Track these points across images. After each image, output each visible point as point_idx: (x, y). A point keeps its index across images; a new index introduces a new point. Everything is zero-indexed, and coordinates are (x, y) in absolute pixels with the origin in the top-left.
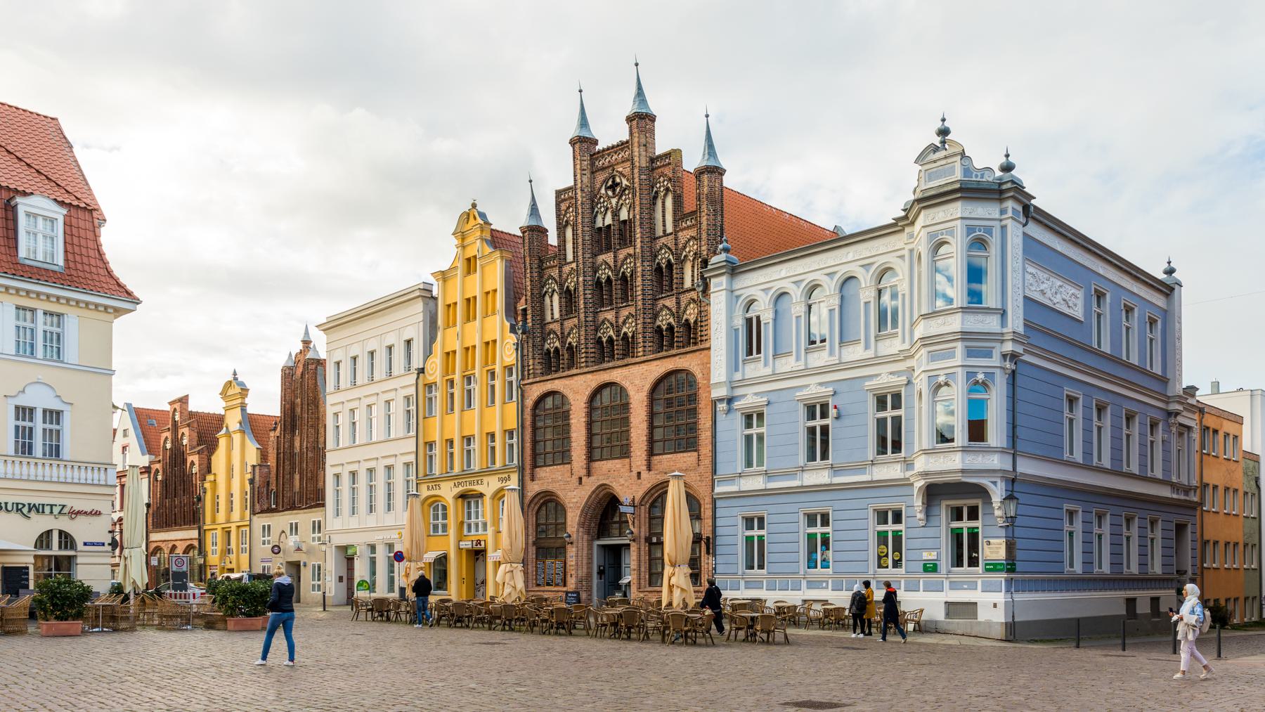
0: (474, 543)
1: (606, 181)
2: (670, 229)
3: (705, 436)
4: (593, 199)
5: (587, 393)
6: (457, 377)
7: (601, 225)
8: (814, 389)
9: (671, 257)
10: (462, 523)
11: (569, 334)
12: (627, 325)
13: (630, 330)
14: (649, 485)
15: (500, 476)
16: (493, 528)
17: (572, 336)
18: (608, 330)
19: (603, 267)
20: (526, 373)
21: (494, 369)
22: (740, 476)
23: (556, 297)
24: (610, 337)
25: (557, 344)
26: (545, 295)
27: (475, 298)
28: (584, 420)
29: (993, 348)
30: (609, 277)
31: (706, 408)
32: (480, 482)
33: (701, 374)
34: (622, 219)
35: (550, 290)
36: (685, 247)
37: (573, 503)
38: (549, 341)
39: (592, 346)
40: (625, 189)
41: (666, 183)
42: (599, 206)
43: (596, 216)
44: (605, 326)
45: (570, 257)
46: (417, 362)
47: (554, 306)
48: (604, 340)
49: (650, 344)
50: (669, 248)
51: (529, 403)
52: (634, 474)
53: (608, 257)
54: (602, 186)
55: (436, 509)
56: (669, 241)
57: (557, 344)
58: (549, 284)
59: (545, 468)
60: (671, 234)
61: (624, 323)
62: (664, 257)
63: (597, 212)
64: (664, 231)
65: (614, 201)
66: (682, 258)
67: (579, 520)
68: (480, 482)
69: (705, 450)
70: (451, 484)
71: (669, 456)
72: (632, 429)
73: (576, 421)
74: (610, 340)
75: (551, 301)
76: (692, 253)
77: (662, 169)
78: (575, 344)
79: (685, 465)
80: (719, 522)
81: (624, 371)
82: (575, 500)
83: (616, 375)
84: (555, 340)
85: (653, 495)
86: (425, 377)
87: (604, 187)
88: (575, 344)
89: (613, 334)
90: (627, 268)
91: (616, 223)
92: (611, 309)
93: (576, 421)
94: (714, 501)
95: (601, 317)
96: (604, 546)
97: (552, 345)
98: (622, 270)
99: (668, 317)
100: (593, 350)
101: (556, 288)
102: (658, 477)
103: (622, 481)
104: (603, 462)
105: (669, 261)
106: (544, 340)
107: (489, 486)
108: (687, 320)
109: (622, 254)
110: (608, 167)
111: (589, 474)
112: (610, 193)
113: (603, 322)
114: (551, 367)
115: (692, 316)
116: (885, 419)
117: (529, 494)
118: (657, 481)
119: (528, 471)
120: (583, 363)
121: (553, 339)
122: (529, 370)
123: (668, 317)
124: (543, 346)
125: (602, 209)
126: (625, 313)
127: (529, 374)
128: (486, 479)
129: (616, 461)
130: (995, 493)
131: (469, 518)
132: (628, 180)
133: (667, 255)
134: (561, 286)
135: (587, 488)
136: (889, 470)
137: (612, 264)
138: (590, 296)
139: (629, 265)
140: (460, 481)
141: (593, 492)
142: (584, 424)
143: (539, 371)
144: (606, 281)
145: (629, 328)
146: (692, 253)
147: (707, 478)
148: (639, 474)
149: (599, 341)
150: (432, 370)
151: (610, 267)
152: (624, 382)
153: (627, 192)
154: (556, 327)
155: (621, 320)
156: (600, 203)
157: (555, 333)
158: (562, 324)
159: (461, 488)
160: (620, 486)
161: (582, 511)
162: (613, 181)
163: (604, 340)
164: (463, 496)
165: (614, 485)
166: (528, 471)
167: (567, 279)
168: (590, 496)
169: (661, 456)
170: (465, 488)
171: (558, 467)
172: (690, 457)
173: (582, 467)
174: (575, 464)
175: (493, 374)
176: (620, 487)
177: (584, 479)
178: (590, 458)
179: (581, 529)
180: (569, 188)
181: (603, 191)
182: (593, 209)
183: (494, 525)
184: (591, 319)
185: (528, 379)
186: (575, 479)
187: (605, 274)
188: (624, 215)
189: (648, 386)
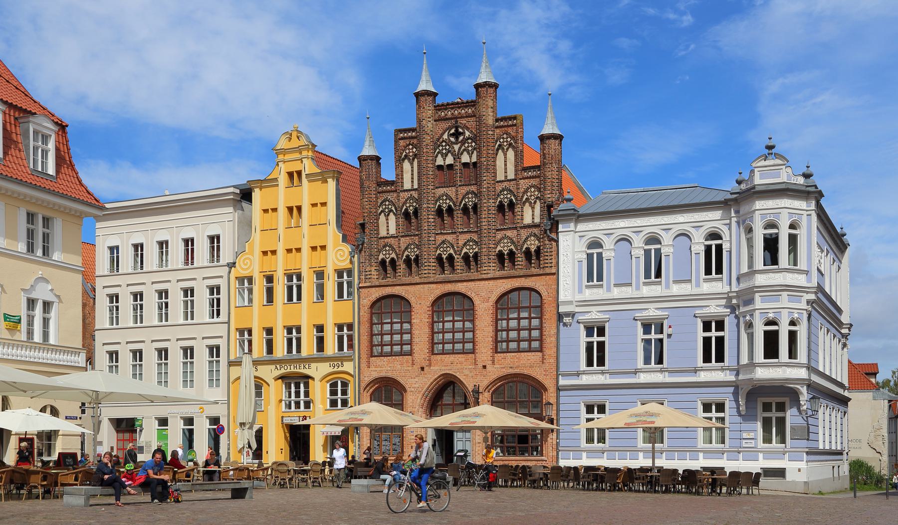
1: (450, 128)
2: (511, 175)
3: (549, 341)
7: (442, 163)
8: (652, 312)
9: (513, 198)
13: (471, 251)
14: (495, 377)
17: (409, 250)
19: (445, 198)
20: (363, 277)
21: (324, 270)
22: (584, 373)
23: (392, 217)
24: (450, 255)
26: (380, 214)
27: (299, 209)
29: (802, 296)
31: (551, 319)
32: (307, 366)
33: (546, 292)
34: (463, 161)
35: (387, 210)
36: (526, 192)
41: (509, 139)
42: (441, 148)
43: (437, 156)
45: (407, 185)
46: (226, 256)
47: (389, 225)
48: (444, 257)
49: (494, 265)
50: (511, 191)
51: (367, 302)
52: (480, 366)
53: (451, 191)
54: (445, 132)
56: (512, 186)
57: (393, 255)
58: (385, 205)
60: (511, 180)
62: (505, 198)
64: (506, 177)
65: (456, 147)
66: (524, 199)
68: (307, 366)
69: (550, 351)
70: (273, 367)
71: (513, 354)
75: (387, 219)
76: (533, 198)
77: (506, 129)
78: (413, 258)
79: (529, 362)
80: (562, 407)
82: (417, 386)
83: (461, 287)
84: (391, 252)
85: (496, 384)
87: (447, 133)
88: (413, 258)
89: (453, 253)
90: (469, 201)
91: (458, 164)
92: (452, 233)
94: (559, 389)
97: (387, 256)
98: (464, 202)
99: (509, 244)
101: (393, 209)
102: (504, 370)
103: (467, 372)
105: (511, 201)
107: (318, 371)
108: (528, 249)
111: (430, 365)
112: (452, 139)
114: (387, 274)
115: (533, 246)
116: (710, 338)
118: (502, 373)
123: (509, 244)
125: (444, 151)
126: (463, 239)
128: (313, 365)
130: (802, 393)
133: (509, 196)
136: (714, 374)
137: (453, 196)
138: (433, 220)
141: (436, 379)
144: (446, 210)
145: (469, 249)
146: (533, 198)
147: (552, 373)
148: (484, 367)
150: (245, 264)
151: (451, 199)
152: (469, 293)
154: (392, 241)
155: (461, 243)
156: (442, 146)
157: (390, 246)
159: (283, 371)
160: (464, 376)
162: (457, 130)
163: (444, 257)
165: (457, 375)
167: (405, 203)
169: (505, 354)
170: (288, 370)
171: (397, 357)
172: (534, 356)
176: (465, 377)
179: (420, 409)
181: (445, 136)
186: (417, 367)
187: (446, 203)
188: (465, 158)
189: (494, 298)
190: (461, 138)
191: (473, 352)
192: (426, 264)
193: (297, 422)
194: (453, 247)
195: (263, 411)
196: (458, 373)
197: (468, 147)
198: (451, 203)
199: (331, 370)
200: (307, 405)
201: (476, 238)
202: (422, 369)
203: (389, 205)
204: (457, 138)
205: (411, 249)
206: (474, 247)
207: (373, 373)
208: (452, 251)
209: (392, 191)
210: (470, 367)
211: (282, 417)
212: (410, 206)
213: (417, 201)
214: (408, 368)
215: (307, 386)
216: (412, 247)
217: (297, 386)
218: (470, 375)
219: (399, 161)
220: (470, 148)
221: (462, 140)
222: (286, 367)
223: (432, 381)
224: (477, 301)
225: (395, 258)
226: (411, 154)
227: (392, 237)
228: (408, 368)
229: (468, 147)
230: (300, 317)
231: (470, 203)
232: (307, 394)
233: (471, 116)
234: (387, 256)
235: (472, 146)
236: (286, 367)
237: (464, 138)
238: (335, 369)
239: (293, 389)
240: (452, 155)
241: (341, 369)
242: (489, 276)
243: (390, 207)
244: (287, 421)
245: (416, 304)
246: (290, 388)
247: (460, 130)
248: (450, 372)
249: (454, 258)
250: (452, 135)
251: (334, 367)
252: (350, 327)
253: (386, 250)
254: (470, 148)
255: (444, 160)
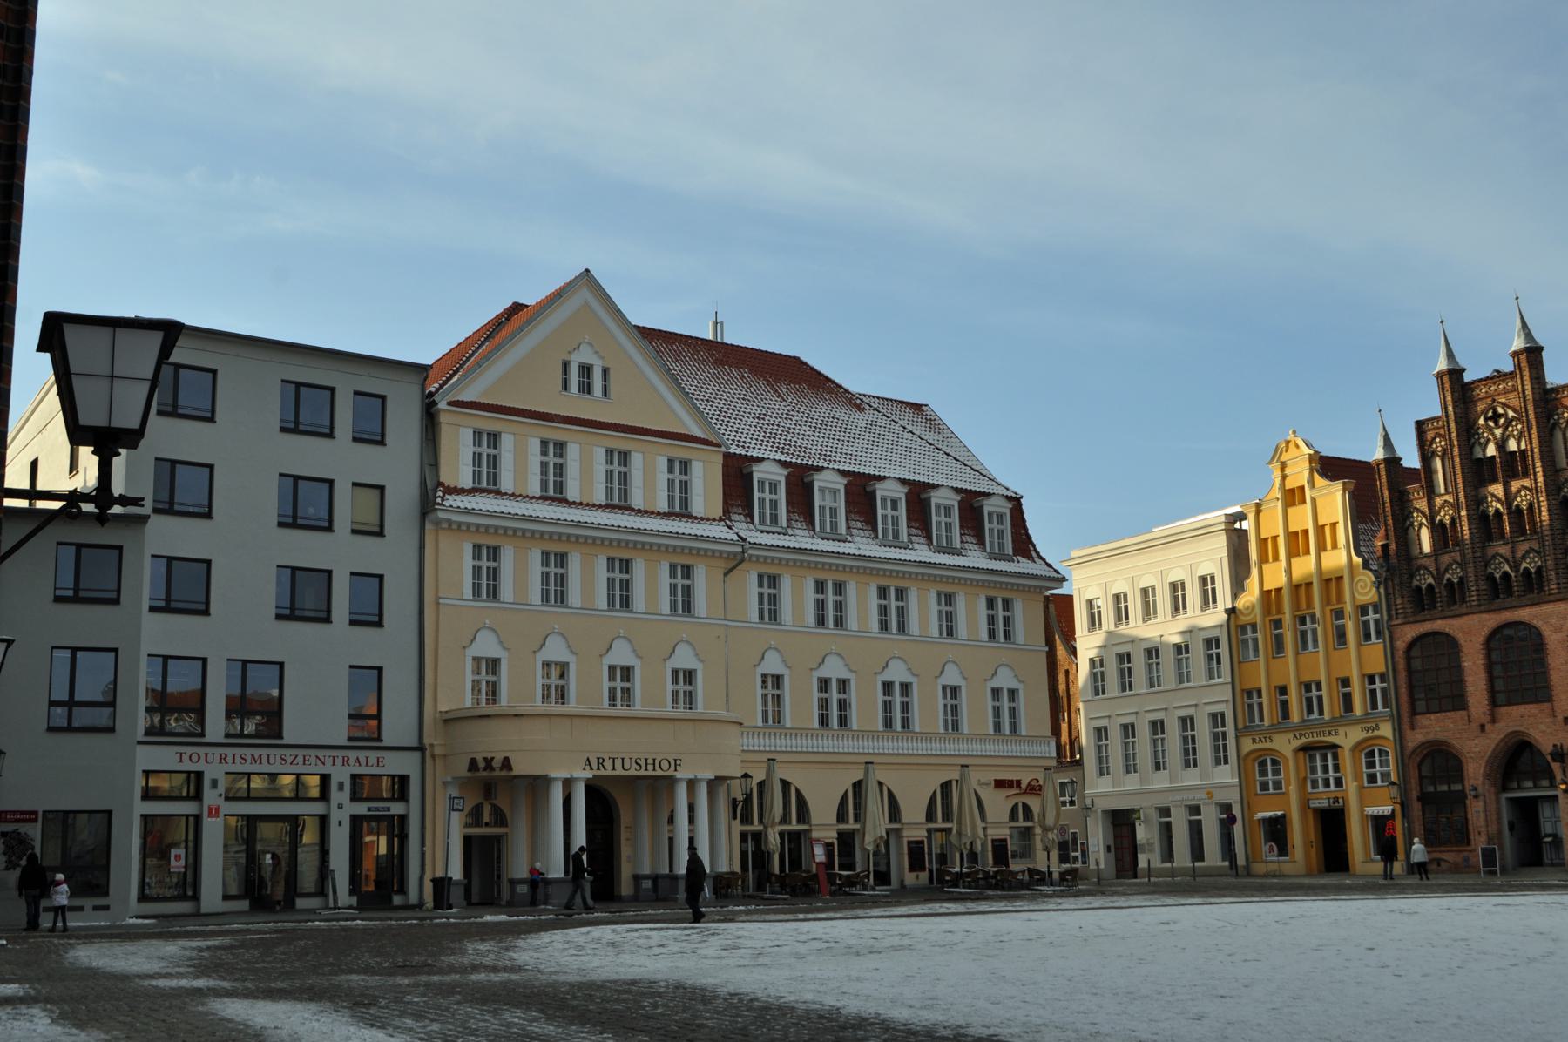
0: (1331, 801)
4: (1468, 432)
5: (1483, 634)
6: (1287, 617)
10: (1305, 779)
11: (1446, 570)
12: (1528, 560)
13: (1533, 565)
15: (1364, 726)
16: (1355, 784)
17: (1450, 572)
18: (1502, 565)
20: (1393, 612)
24: (1506, 575)
25: (1430, 580)
27: (1306, 532)
28: (1482, 662)
30: (1497, 510)
37: (1474, 753)
38: (1418, 578)
39: (1482, 583)
40: (1512, 421)
43: (1473, 446)
44: (1497, 561)
48: (1498, 576)
51: (1401, 645)
55: (1263, 764)
57: (1430, 580)
59: (1429, 715)
61: (1524, 558)
63: (1474, 443)
65: (1498, 432)
67: (1485, 771)
70: (1291, 736)
72: (1551, 672)
73: (1470, 664)
74: (1506, 575)
78: (1456, 581)
81: (1536, 610)
82: (1477, 750)
83: (1523, 614)
84: (1426, 576)
86: (1237, 617)
88: (1456, 581)
90: (1522, 501)
93: (1470, 664)
95: (1491, 552)
96: (1511, 799)
97: (1423, 582)
100: (1485, 587)
101: (1424, 521)
103: (1543, 727)
104: (1511, 707)
106: (1412, 576)
107: (1348, 738)
109: (1515, 485)
110: (1486, 398)
111: (1494, 721)
112: (1491, 424)
113: (1494, 557)
117: (1410, 744)
119: (1406, 719)
120: (1473, 601)
121: (1424, 574)
122: (1396, 610)
124: (1411, 582)
125: (1482, 440)
127: (1397, 614)
128: (1341, 731)
129: (1531, 706)
131: (1313, 770)
132: (1515, 411)
134: (1432, 519)
135: (1493, 736)
138: (1475, 531)
139: (1524, 498)
140: (1303, 732)
142: (1482, 667)
143: (1409, 611)
144: (1493, 515)
149: (1491, 578)
151: (1498, 500)
152: (1535, 622)
153: (1514, 423)
154: (1425, 562)
155: (1519, 555)
157: (1426, 568)
158: (1436, 560)
159: (1304, 740)
161: (1487, 762)
163: (1498, 576)
164: (1305, 748)
165: (1531, 732)
166: (1406, 719)
168: (1497, 745)
170: (1311, 739)
173: (1484, 713)
174: (1473, 710)
175: (1339, 614)
176: (1540, 734)
177: (1488, 727)
178: (1494, 703)
179: (1487, 781)
180: (1437, 419)
181: (1481, 421)
182: (1469, 440)
183: (1356, 781)
184: (1479, 554)
185: (1397, 618)
186: (1475, 725)
188: (1512, 446)
190: (1502, 421)
191: (1549, 699)
192: (1473, 589)
193: (1324, 803)
194: (1507, 560)
195: (1283, 793)
196: (1531, 730)
197: (1513, 431)
198: (1499, 506)
199: (1364, 735)
200: (1339, 782)
201: (1536, 547)
202: (1482, 727)
203: (1418, 516)
204: (1496, 423)
205: (1453, 569)
206: (1536, 559)
207: (1417, 736)
208: (1507, 568)
209: (1420, 499)
210: (1547, 720)
211: (1308, 800)
212: (1444, 516)
213: (1452, 505)
214: (1464, 727)
215: (1335, 757)
216: (1454, 567)
217: (1325, 759)
218: (1549, 731)
219: (1426, 458)
220: (1515, 433)
221: (1503, 424)
222: (1307, 735)
223: (1496, 742)
224: (1547, 632)
225: (1433, 582)
226: (1439, 449)
227: (1427, 556)
228: (1464, 727)
229: (1513, 431)
230: (1351, 671)
231: (1524, 503)
232: (1337, 768)
233: (1512, 391)
234: (1423, 582)
235: (1517, 430)
236: (1307, 735)
237: (1505, 421)
238: (1370, 734)
239: (1319, 763)
240: (1496, 444)
241: (1376, 733)
242: (1558, 597)
243: (1419, 519)
244: (1315, 804)
245: (1466, 641)
246: (1326, 760)
247: (1500, 411)
248: (1521, 729)
249: (1510, 576)
250: (1490, 418)
251: (1368, 731)
252: (1383, 678)
253: (1420, 575)
254: (1515, 433)
255: (1484, 451)
